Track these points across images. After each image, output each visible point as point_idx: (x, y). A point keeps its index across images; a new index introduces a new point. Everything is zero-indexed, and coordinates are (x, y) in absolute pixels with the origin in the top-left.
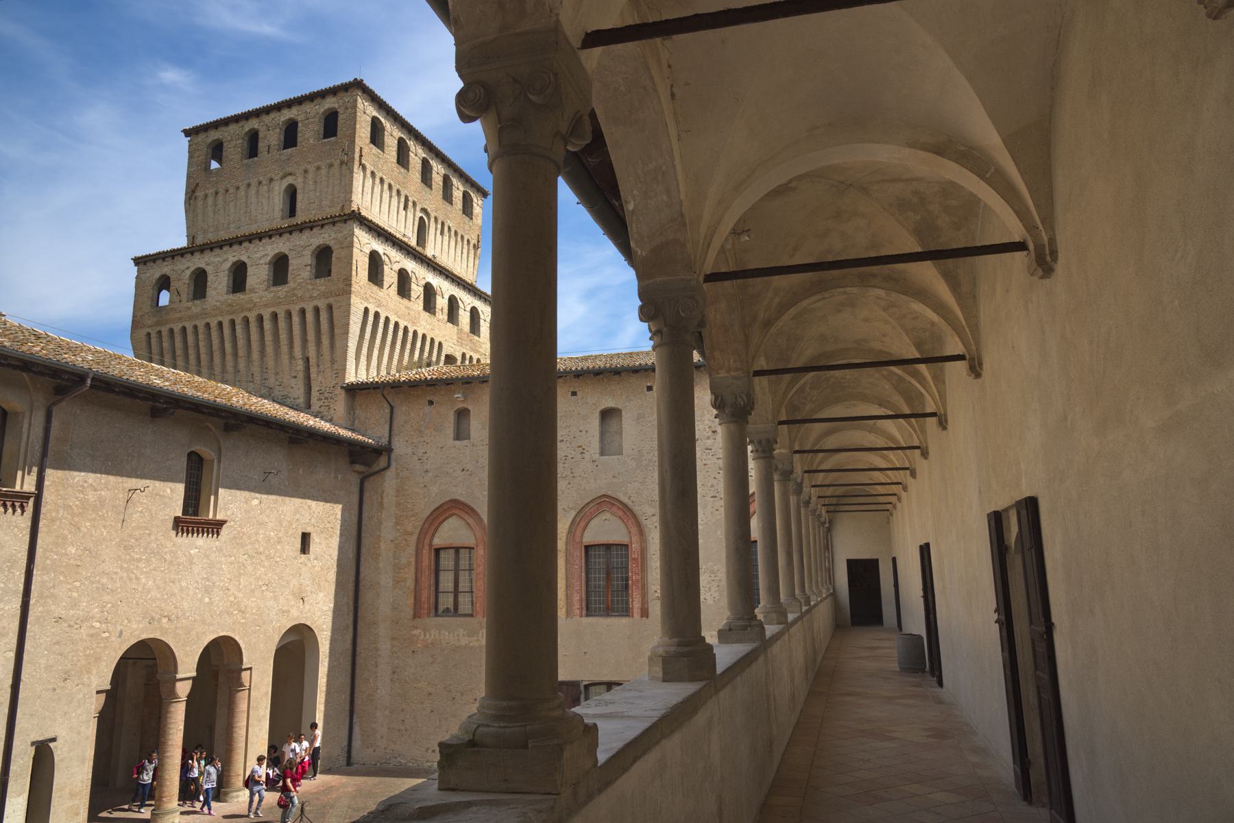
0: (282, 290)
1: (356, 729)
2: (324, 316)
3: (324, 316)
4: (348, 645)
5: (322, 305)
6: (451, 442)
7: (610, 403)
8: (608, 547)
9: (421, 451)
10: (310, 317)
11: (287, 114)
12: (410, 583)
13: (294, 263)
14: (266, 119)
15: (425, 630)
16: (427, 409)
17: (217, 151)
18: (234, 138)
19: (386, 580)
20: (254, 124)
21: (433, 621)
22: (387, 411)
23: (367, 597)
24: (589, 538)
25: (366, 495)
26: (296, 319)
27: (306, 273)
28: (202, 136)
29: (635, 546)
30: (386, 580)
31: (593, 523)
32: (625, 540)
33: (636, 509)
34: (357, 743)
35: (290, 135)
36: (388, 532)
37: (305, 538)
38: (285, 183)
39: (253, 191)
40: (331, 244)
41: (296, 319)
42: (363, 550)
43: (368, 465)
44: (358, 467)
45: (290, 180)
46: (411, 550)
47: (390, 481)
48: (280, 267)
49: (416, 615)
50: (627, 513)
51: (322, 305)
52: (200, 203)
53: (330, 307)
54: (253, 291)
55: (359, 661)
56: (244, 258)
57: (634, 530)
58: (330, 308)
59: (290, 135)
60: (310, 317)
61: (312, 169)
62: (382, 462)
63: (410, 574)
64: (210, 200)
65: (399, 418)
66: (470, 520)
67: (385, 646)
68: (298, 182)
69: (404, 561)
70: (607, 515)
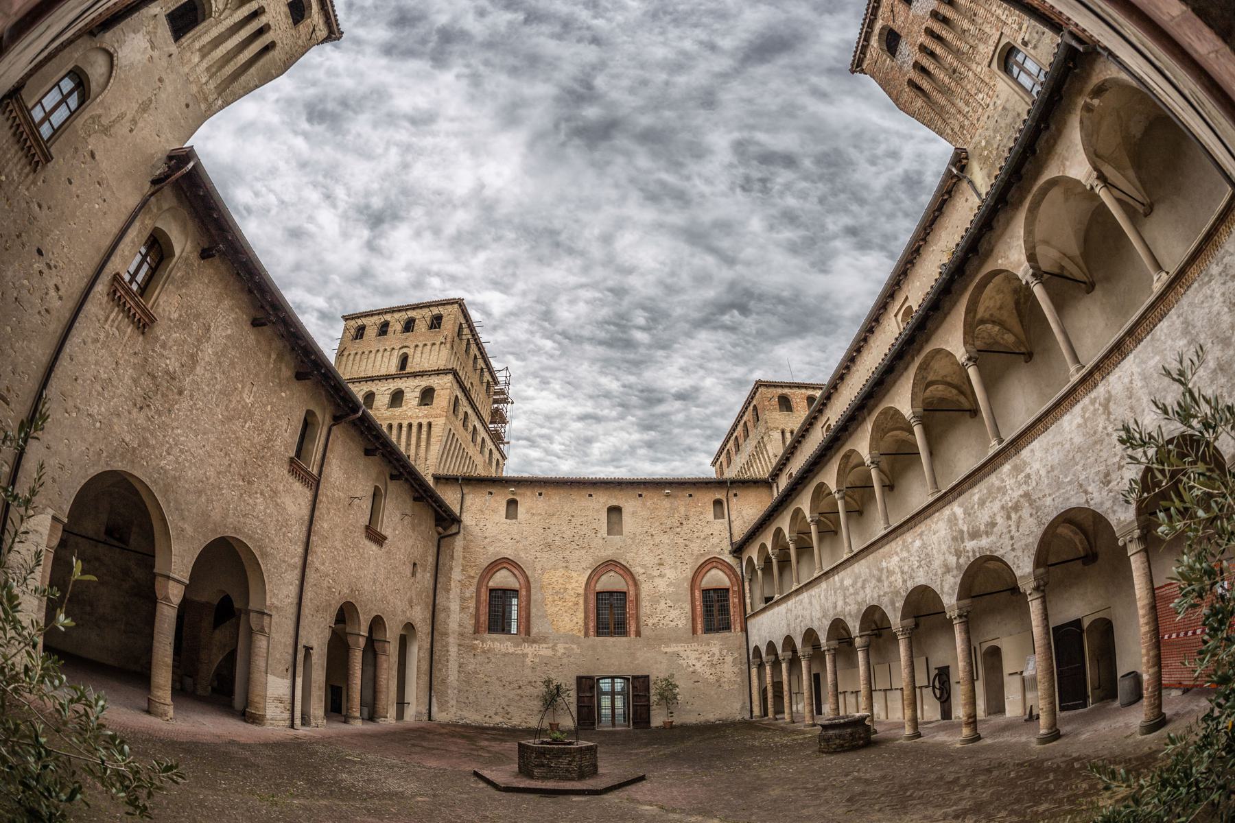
0: (397, 411)
1: (434, 700)
2: (424, 429)
3: (424, 429)
4: (428, 646)
5: (425, 422)
6: (504, 520)
7: (614, 502)
8: (611, 593)
9: (482, 524)
10: (414, 429)
11: (411, 314)
12: (472, 610)
13: (407, 396)
14: (397, 315)
15: (483, 642)
16: (487, 497)
17: (361, 330)
18: (372, 323)
19: (454, 606)
20: (388, 317)
21: (487, 636)
22: (459, 496)
23: (441, 616)
24: (599, 588)
25: (442, 549)
26: (405, 429)
27: (415, 402)
28: (352, 323)
29: (632, 593)
30: (454, 606)
31: (603, 578)
32: (625, 589)
33: (632, 570)
34: (435, 709)
35: (409, 326)
36: (457, 575)
37: (415, 564)
38: (402, 352)
39: (380, 355)
40: (435, 386)
41: (405, 429)
42: (439, 586)
43: (445, 529)
44: (440, 529)
45: (405, 350)
46: (473, 589)
47: (459, 542)
48: (397, 398)
49: (476, 631)
50: (626, 571)
51: (425, 422)
52: (344, 358)
53: (430, 424)
54: (377, 409)
55: (435, 657)
56: (374, 390)
57: (631, 583)
58: (430, 424)
59: (409, 326)
60: (414, 429)
61: (421, 345)
62: (454, 529)
63: (472, 604)
64: (351, 357)
65: (469, 500)
66: (516, 572)
67: (453, 650)
68: (410, 352)
69: (468, 595)
70: (612, 573)
